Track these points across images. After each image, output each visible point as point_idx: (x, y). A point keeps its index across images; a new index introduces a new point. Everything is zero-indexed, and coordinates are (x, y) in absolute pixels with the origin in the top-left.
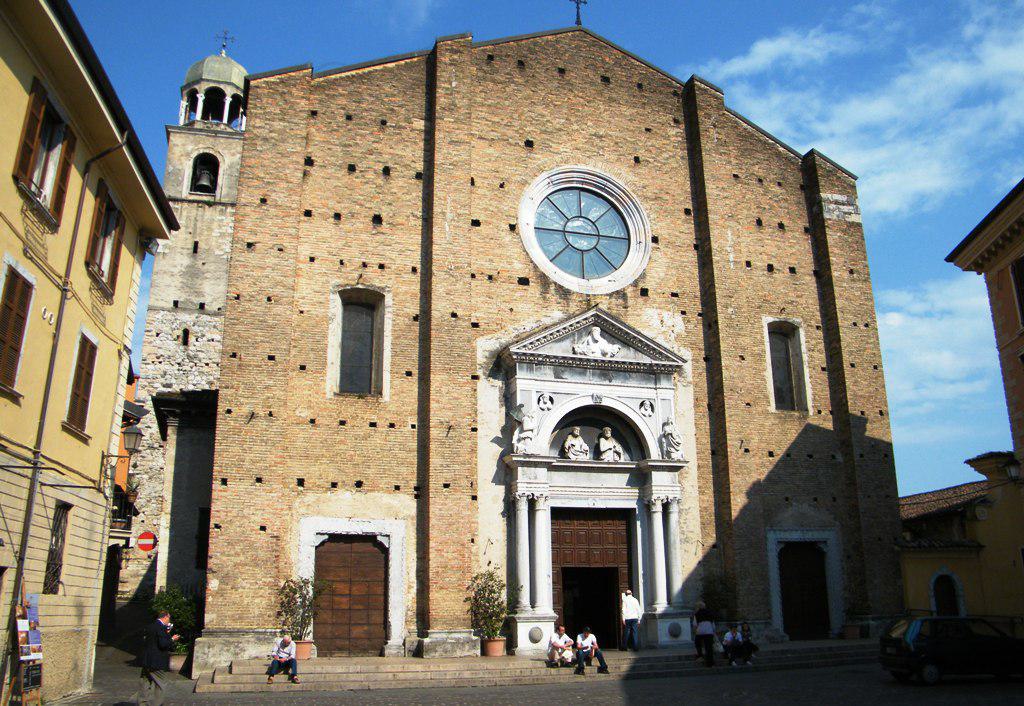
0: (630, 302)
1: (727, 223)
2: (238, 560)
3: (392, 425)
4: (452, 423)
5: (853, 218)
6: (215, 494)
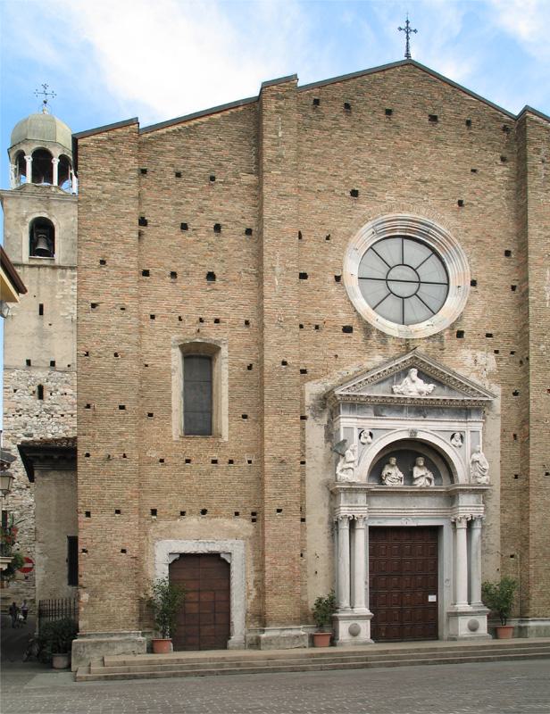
0: (446, 345)
3: (231, 462)
4: (283, 458)
6: (81, 525)
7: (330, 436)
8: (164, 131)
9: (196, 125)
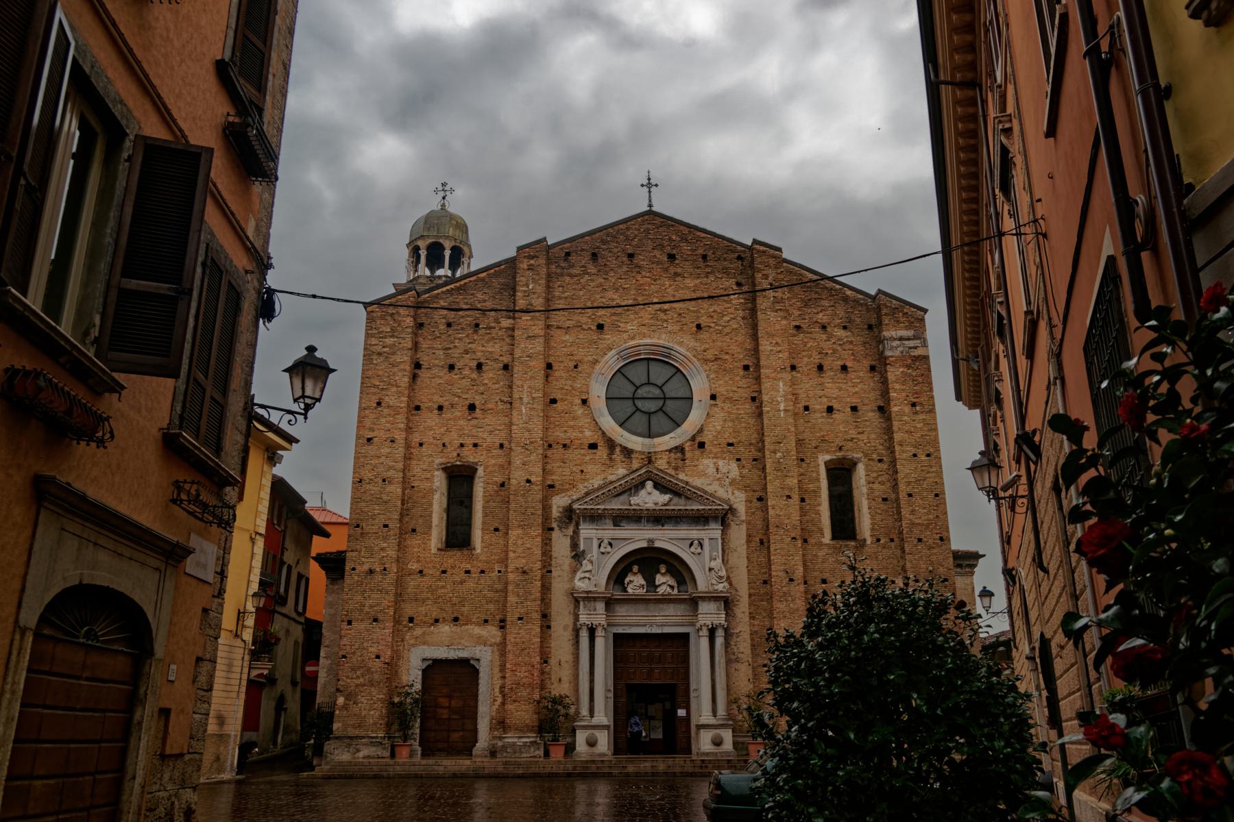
0: (688, 455)
2: (356, 681)
3: (483, 572)
4: (525, 568)
7: (574, 545)
8: (440, 291)
9: (465, 284)
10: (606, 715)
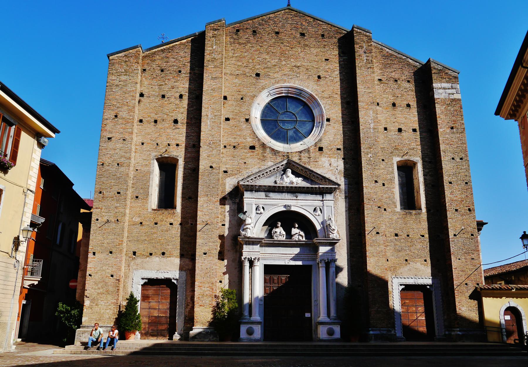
0: (312, 155)
1: (370, 107)
2: (99, 291)
5: (458, 96)
6: (89, 260)
9: (173, 46)
10: (260, 315)
